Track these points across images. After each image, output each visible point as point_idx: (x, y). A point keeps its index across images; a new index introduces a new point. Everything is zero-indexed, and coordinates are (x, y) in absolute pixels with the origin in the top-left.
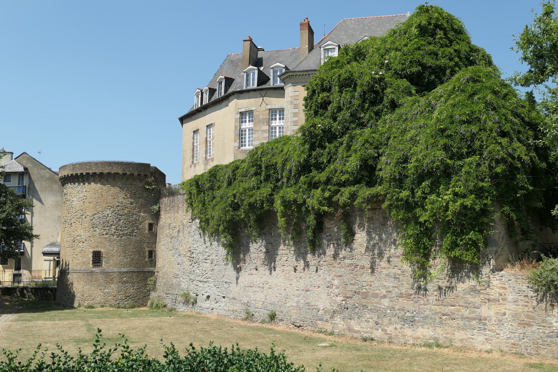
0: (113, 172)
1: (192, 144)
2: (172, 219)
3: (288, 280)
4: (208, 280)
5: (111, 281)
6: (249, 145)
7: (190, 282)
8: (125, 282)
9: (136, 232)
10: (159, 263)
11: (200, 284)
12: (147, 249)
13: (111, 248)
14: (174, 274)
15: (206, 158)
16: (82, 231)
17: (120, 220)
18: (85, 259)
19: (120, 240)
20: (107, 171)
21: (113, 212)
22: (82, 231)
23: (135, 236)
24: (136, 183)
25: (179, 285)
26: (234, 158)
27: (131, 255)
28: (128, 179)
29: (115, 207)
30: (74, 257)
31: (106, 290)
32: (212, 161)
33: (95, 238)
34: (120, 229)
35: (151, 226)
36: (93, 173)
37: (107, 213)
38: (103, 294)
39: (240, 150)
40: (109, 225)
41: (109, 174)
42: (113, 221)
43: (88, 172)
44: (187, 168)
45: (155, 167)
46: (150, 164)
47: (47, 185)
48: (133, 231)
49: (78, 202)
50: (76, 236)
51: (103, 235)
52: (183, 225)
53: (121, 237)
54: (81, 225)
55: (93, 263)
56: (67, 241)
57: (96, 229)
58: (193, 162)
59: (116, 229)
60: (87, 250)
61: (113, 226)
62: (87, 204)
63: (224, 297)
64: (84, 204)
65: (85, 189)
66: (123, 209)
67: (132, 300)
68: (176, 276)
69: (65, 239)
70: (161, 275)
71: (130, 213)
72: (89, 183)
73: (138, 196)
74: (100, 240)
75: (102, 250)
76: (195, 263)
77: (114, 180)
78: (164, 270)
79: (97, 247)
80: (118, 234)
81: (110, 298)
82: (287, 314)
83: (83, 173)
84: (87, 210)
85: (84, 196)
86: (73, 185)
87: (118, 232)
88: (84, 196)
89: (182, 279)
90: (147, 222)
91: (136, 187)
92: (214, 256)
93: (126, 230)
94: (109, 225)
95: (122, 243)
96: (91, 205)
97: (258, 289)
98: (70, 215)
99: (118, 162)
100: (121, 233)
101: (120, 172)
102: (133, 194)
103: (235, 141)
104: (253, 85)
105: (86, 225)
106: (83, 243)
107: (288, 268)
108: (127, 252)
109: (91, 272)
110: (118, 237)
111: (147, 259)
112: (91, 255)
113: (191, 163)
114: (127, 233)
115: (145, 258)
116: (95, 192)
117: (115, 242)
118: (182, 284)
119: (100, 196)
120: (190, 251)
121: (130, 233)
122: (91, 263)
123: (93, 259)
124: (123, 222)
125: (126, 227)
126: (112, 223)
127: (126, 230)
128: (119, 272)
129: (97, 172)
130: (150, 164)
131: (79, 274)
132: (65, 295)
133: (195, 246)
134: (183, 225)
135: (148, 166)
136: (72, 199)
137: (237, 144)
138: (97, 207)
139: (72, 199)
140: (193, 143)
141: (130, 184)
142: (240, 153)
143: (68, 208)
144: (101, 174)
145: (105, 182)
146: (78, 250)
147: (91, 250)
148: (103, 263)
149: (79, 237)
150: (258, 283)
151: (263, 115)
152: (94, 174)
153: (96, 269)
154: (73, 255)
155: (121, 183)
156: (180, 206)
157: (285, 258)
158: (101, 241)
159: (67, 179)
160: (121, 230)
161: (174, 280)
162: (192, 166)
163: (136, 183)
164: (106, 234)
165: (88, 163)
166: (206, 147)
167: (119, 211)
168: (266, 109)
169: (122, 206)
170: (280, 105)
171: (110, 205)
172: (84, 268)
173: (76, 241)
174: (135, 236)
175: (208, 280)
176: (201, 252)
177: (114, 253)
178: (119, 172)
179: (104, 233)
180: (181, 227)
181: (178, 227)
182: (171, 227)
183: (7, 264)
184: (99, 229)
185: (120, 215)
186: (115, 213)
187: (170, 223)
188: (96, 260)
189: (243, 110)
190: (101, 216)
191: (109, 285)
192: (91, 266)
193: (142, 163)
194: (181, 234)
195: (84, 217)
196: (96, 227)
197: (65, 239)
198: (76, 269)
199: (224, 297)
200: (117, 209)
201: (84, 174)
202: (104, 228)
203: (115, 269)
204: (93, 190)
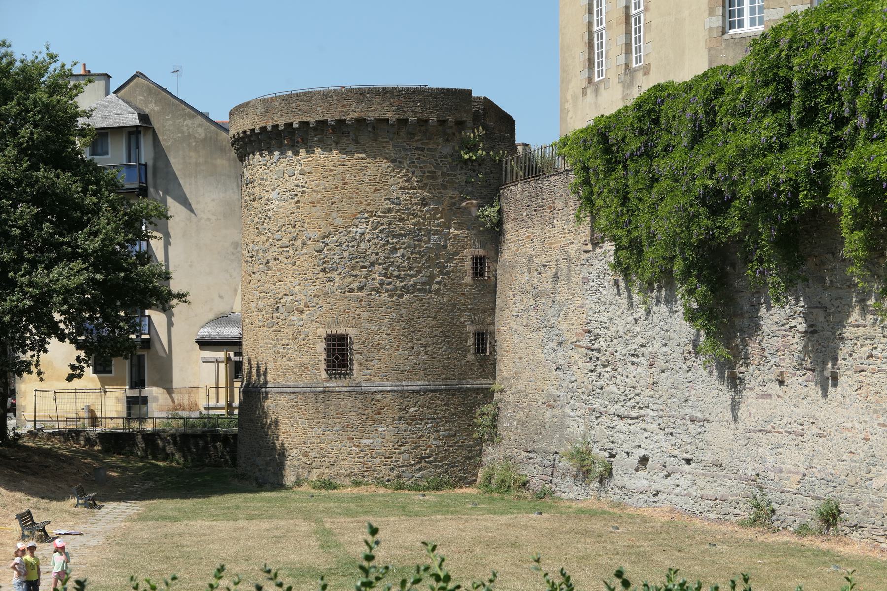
0: (371, 116)
1: (586, 28)
2: (537, 242)
3: (875, 411)
4: (642, 412)
6: (753, 23)
7: (593, 418)
9: (439, 283)
10: (506, 366)
11: (621, 425)
12: (470, 328)
13: (374, 327)
14: (548, 396)
15: (627, 66)
16: (296, 281)
17: (394, 250)
18: (306, 358)
19: (398, 304)
20: (356, 115)
21: (375, 228)
22: (296, 281)
23: (437, 292)
24: (435, 146)
25: (561, 426)
26: (710, 62)
27: (427, 346)
28: (411, 135)
29: (379, 214)
30: (278, 353)
31: (364, 441)
32: (644, 74)
33: (332, 301)
34: (396, 273)
35: (478, 263)
36: (318, 122)
37: (360, 231)
39: (726, 37)
40: (367, 264)
41: (361, 122)
42: (377, 254)
43: (304, 119)
44: (575, 98)
45: (486, 98)
46: (470, 92)
47: (201, 160)
48: (431, 277)
49: (282, 204)
50: (280, 296)
51: (351, 290)
52: (569, 260)
53: (400, 296)
54: (294, 264)
55: (328, 366)
56: (259, 310)
57: (333, 275)
58: (590, 80)
59: (385, 275)
61: (377, 267)
62: (305, 209)
63: (688, 461)
64: (298, 208)
65: (298, 168)
66: (401, 220)
67: (436, 466)
68: (552, 403)
69: (253, 305)
70: (511, 399)
71: (420, 229)
72: (310, 150)
73: (440, 180)
74: (343, 305)
75: (352, 332)
76: (605, 366)
77: (376, 140)
78: (520, 385)
79: (338, 323)
80: (390, 287)
81: (377, 461)
82: (871, 510)
83: (291, 124)
84: (306, 225)
85: (297, 186)
86: (267, 157)
87: (390, 284)
88: (297, 186)
89: (568, 410)
90: (468, 253)
91: (433, 156)
92: (657, 345)
93: (412, 276)
94: (367, 264)
95: (404, 312)
96: (317, 211)
97: (786, 439)
98: (262, 238)
99: (384, 89)
100: (399, 284)
101: (391, 116)
102: (428, 177)
103: (711, 13)
105: (305, 264)
106: (301, 312)
107: (874, 379)
108: (417, 336)
109: (324, 392)
110: (390, 296)
111: (470, 357)
112: (321, 347)
113: (585, 83)
114: (414, 286)
115: (466, 352)
116: (325, 174)
117: (384, 310)
118: (569, 422)
119: (340, 185)
120: (590, 332)
121: (424, 284)
122: (323, 366)
123: (328, 355)
124: (403, 256)
125: (411, 269)
126: (373, 257)
127: (412, 276)
128: (398, 391)
129: (329, 117)
130: (470, 92)
131: (293, 396)
132: (259, 454)
133: (604, 317)
134: (569, 260)
135: (464, 95)
136: (267, 195)
137: (717, 22)
138: (334, 214)
139: (267, 195)
140: (590, 24)
141: (417, 149)
142: (728, 46)
143: (256, 219)
144: (341, 122)
145: (352, 147)
146: (289, 331)
147: (322, 333)
148: (356, 367)
149: (289, 298)
150: (785, 420)
152: (322, 123)
153: (338, 385)
154: (275, 346)
155: (394, 146)
156: (559, 205)
157: (866, 349)
158: (346, 307)
159: (251, 142)
160: (398, 277)
161: (548, 414)
162: (589, 91)
163: (435, 146)
164: (360, 289)
165: (305, 94)
166: (628, 33)
167: (390, 224)
169: (398, 211)
171: (368, 208)
172: (305, 380)
173: (282, 310)
174: (437, 292)
175: (642, 412)
176: (621, 333)
177: (383, 340)
178: (388, 115)
179: (355, 285)
180: (563, 265)
181: (553, 264)
182: (534, 266)
183: (110, 372)
184: (339, 274)
185: (394, 237)
186: (382, 231)
187: (532, 256)
188: (337, 358)
190: (343, 239)
191: (372, 428)
192: (324, 374)
193: (448, 90)
194: (562, 283)
195: (298, 243)
196: (332, 270)
197: (253, 305)
198: (284, 383)
199: (688, 461)
200: (385, 220)
201: (295, 125)
202: (354, 273)
203: (387, 383)
204: (320, 168)
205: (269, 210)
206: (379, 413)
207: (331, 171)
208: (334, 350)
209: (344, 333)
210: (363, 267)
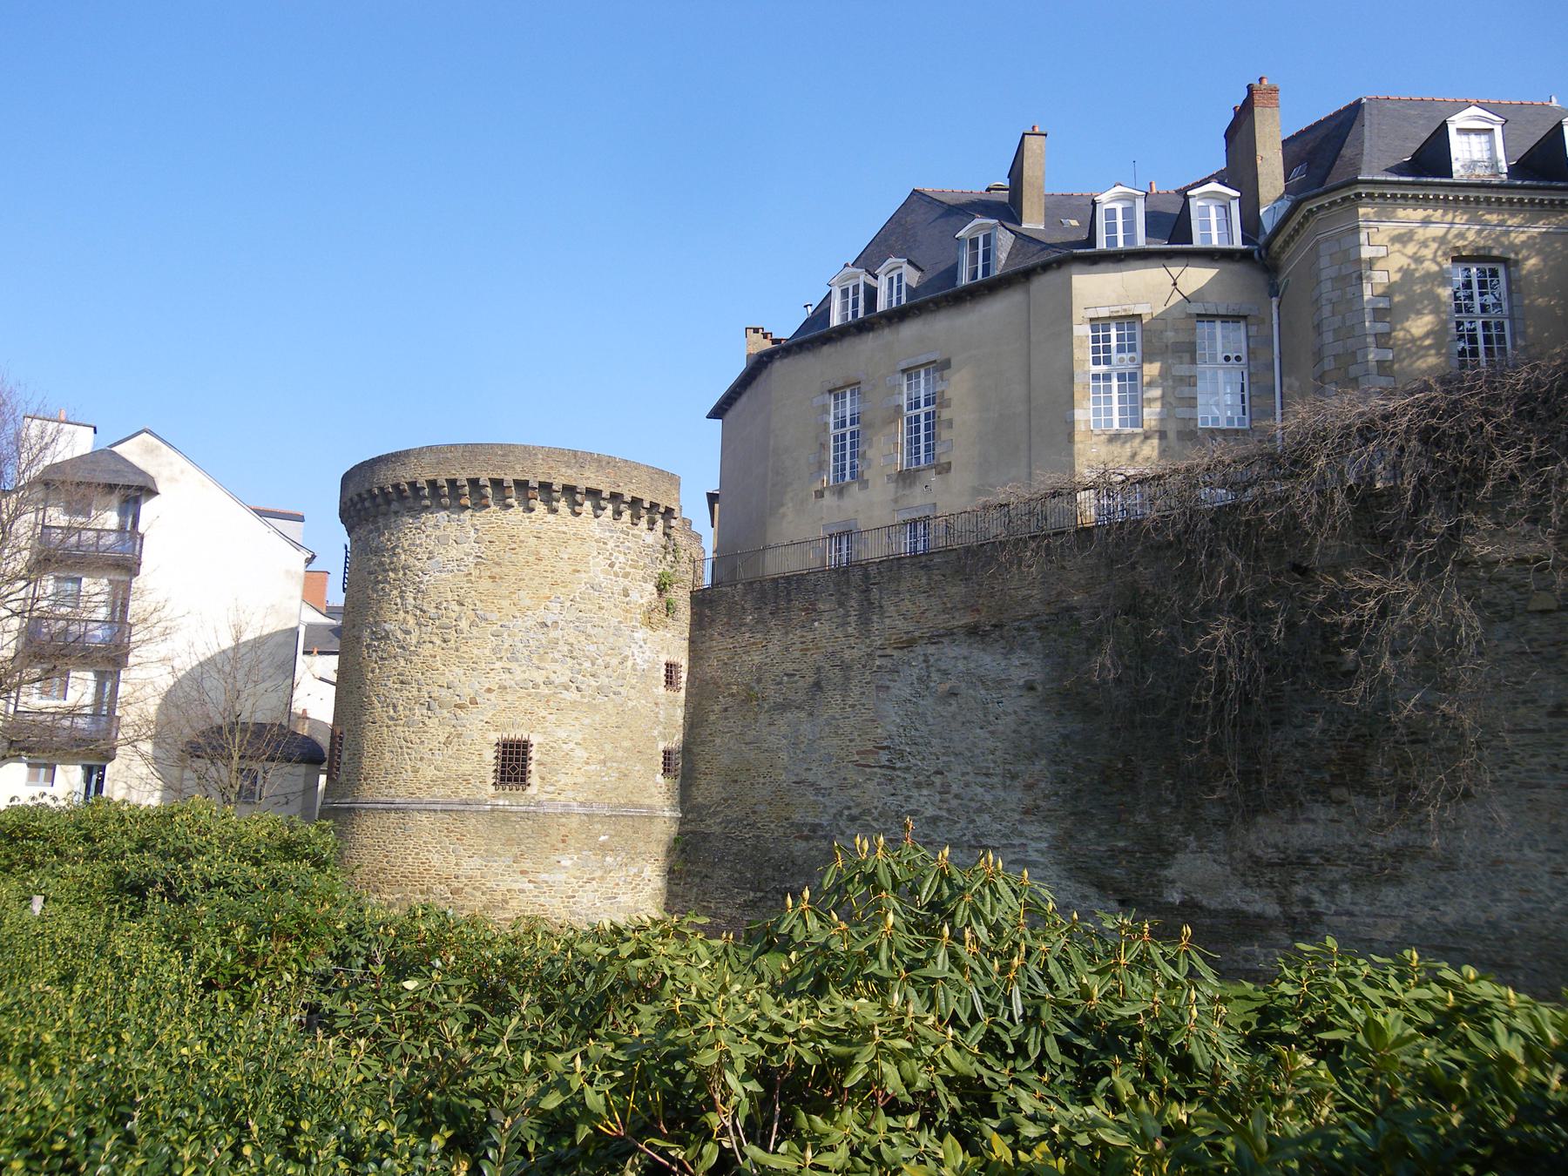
5: (562, 845)
8: (604, 849)
18: (466, 768)
31: (544, 876)
38: (531, 885)
43: (496, 476)
60: (476, 736)
70: (717, 829)
74: (526, 704)
90: (664, 658)
104: (1129, 238)
105: (475, 651)
112: (490, 755)
116: (514, 546)
117: (575, 714)
119: (532, 559)
134: (845, 667)
141: (622, 532)
147: (494, 737)
149: (444, 692)
151: (1176, 331)
168: (1189, 316)
170: (1231, 308)
177: (572, 750)
189: (1104, 313)
192: (492, 789)
196: (513, 659)
198: (428, 799)
205: (421, 582)
206: (564, 841)
207: (522, 542)
208: (511, 760)
209: (525, 737)
210: (555, 661)
